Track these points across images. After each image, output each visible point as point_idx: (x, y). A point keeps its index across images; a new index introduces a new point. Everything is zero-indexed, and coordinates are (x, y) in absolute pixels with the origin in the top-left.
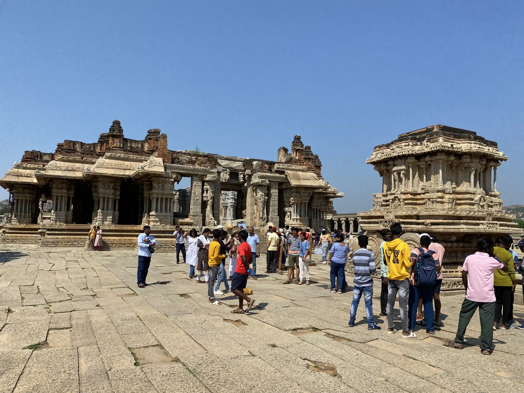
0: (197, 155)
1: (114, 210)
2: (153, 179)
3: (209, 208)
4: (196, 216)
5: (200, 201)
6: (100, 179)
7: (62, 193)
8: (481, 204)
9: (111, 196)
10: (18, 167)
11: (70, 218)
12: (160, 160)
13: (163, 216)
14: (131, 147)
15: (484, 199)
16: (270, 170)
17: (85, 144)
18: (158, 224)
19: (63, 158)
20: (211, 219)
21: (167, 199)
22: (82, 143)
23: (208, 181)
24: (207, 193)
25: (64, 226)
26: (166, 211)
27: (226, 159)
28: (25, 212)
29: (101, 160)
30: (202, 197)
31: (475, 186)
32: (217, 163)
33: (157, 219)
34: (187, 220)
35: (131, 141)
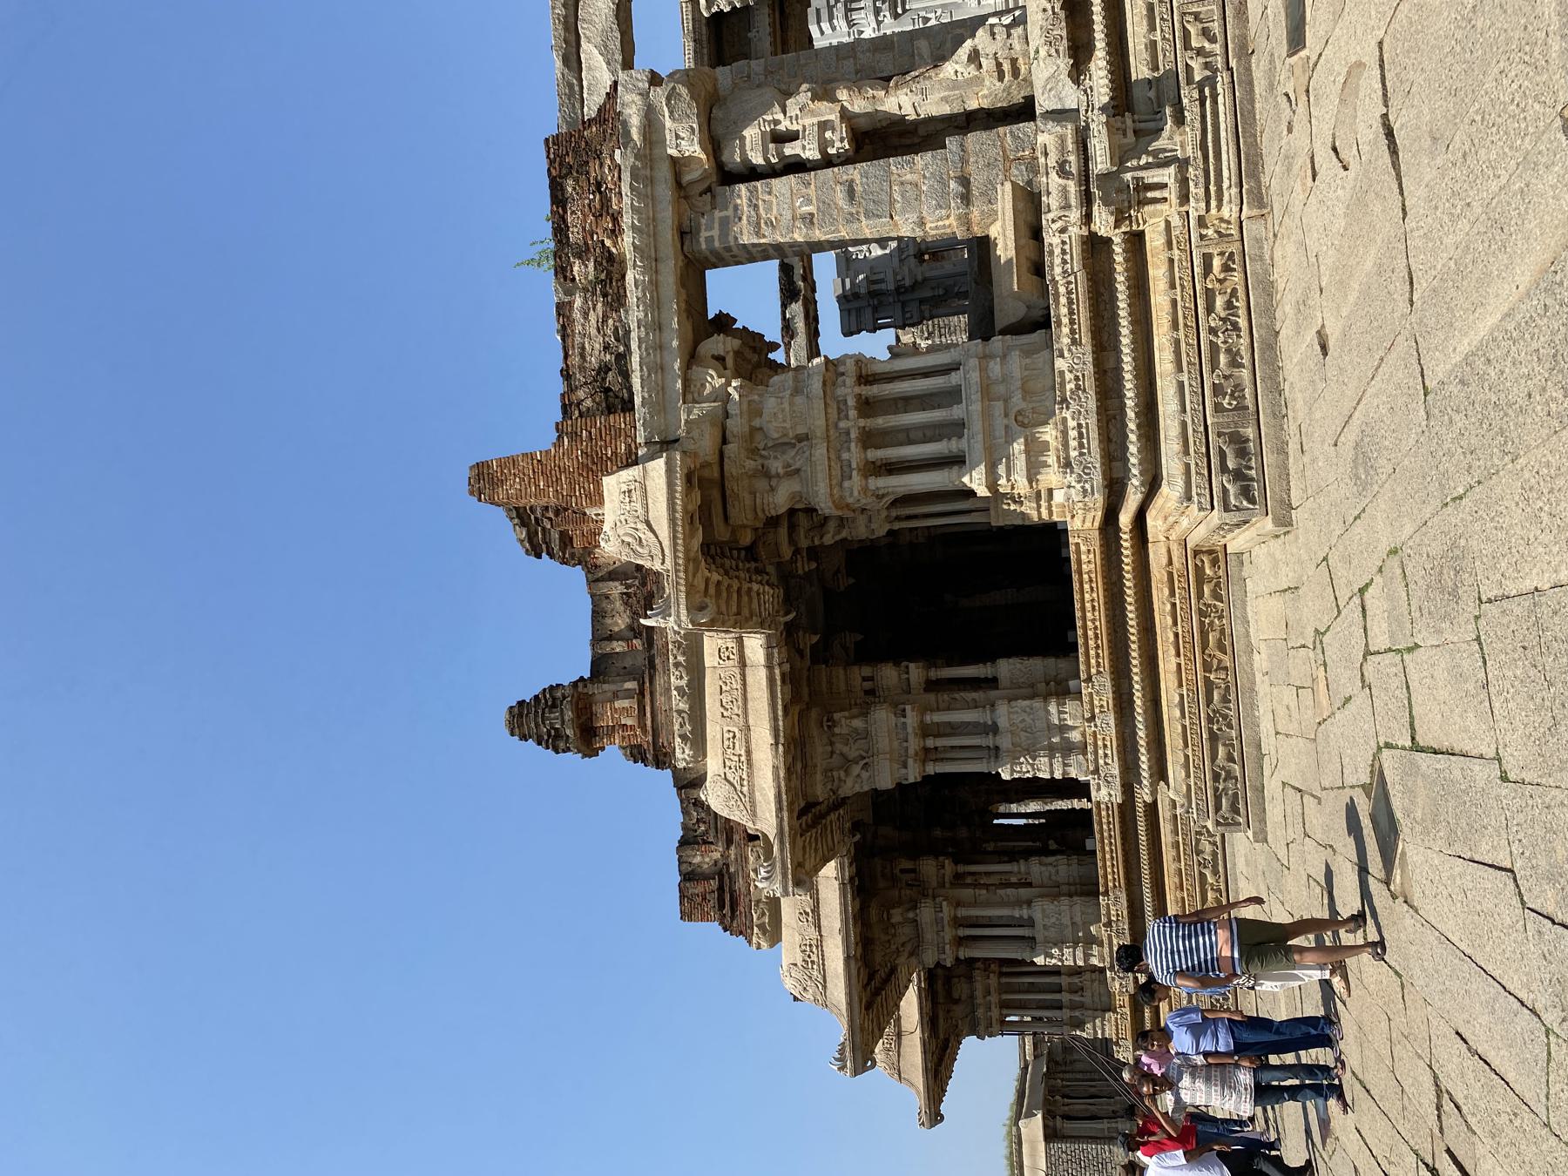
0: (563, 251)
1: (993, 682)
3: (901, 102)
4: (965, 181)
5: (854, 172)
6: (820, 792)
7: (938, 921)
9: (912, 719)
11: (1063, 869)
12: (613, 484)
13: (987, 415)
17: (685, 827)
18: (1049, 434)
19: (761, 927)
20: (974, 57)
21: (868, 407)
22: (684, 843)
23: (714, 143)
24: (792, 137)
25: (1114, 905)
27: (573, 60)
30: (827, 162)
32: (609, 114)
33: (1018, 447)
35: (601, 636)
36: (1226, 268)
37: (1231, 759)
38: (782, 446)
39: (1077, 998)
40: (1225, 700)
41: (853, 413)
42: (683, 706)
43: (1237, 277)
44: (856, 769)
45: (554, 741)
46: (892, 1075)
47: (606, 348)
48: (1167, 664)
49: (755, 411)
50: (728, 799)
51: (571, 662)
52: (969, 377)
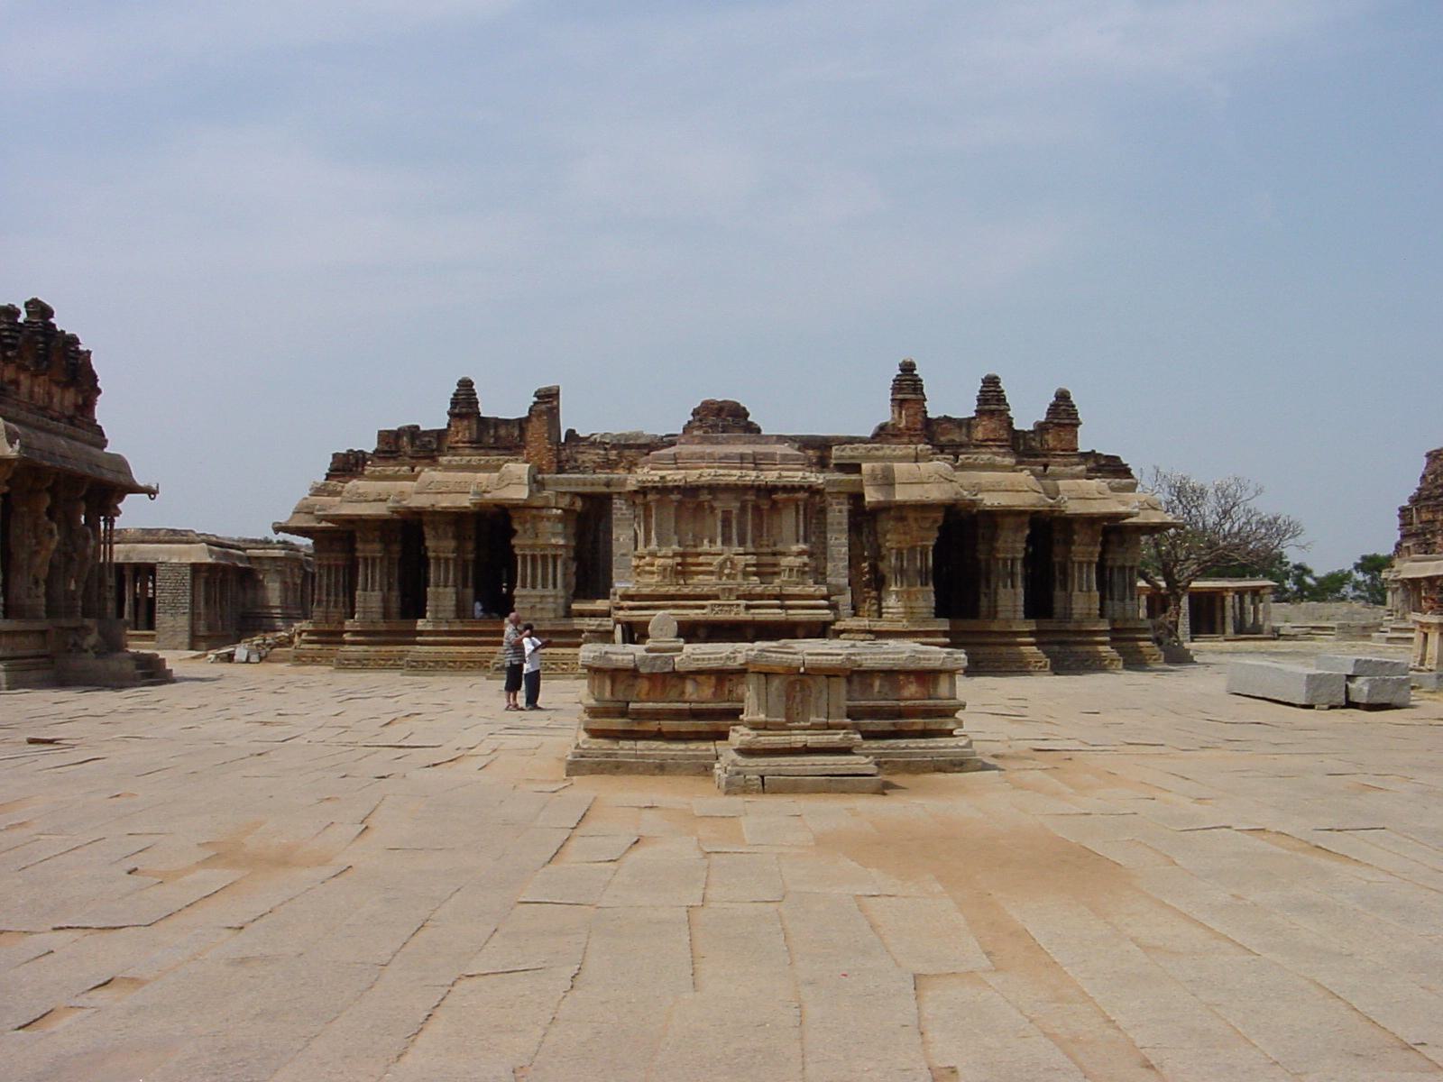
1: (465, 585)
2: (511, 513)
7: (374, 551)
8: (726, 571)
9: (451, 555)
10: (318, 491)
13: (537, 596)
14: (497, 438)
15: (731, 562)
16: (822, 464)
21: (544, 557)
26: (544, 586)
28: (337, 595)
29: (429, 474)
31: (727, 540)
34: (601, 605)
35: (498, 423)
36: (563, 669)
37: (430, 667)
38: (535, 528)
39: (332, 604)
40: (450, 667)
41: (542, 553)
42: (464, 462)
43: (561, 672)
44: (433, 533)
45: (455, 403)
46: (296, 508)
47: (584, 462)
48: (465, 649)
49: (548, 519)
50: (424, 482)
51: (488, 408)
52: (550, 591)
